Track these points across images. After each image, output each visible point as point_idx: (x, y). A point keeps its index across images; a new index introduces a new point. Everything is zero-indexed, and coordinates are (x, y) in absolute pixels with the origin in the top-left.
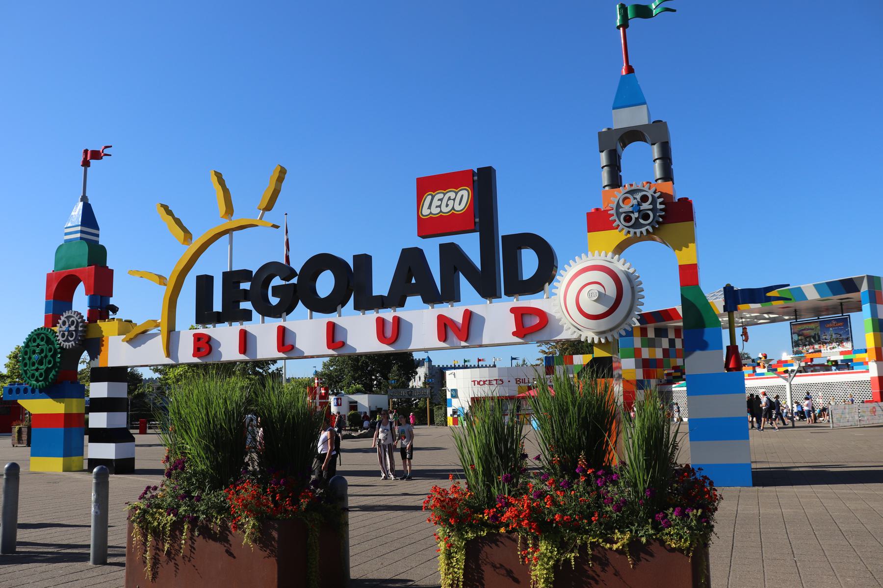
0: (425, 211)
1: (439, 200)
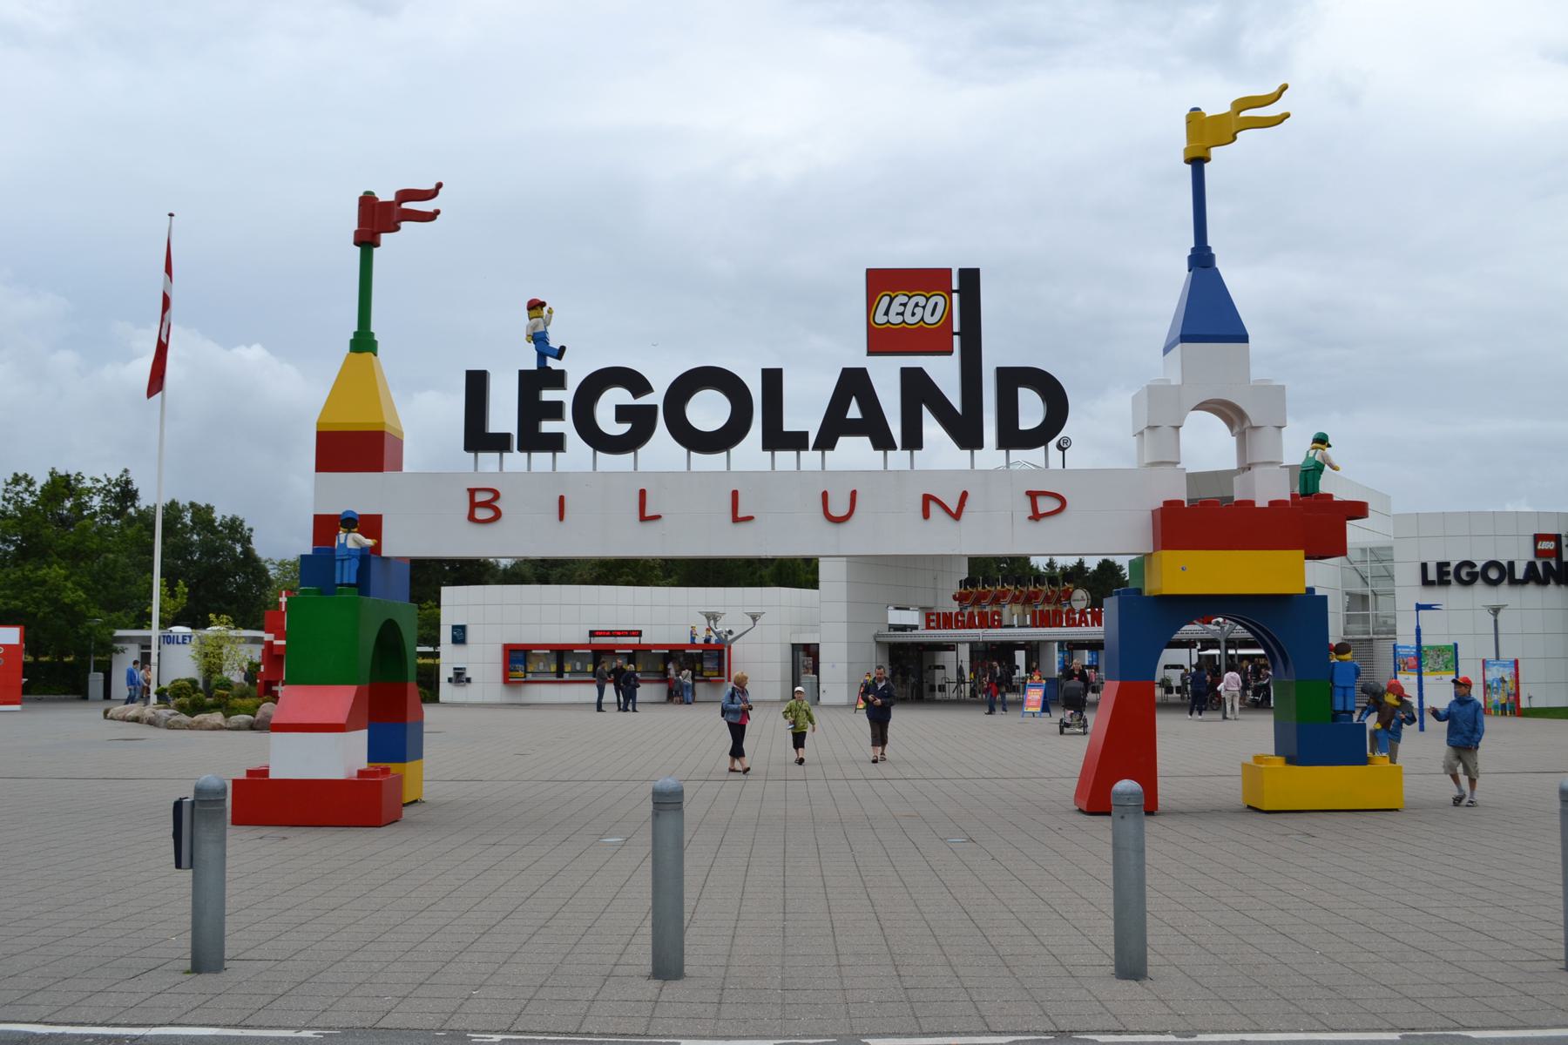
0: (880, 318)
1: (901, 304)
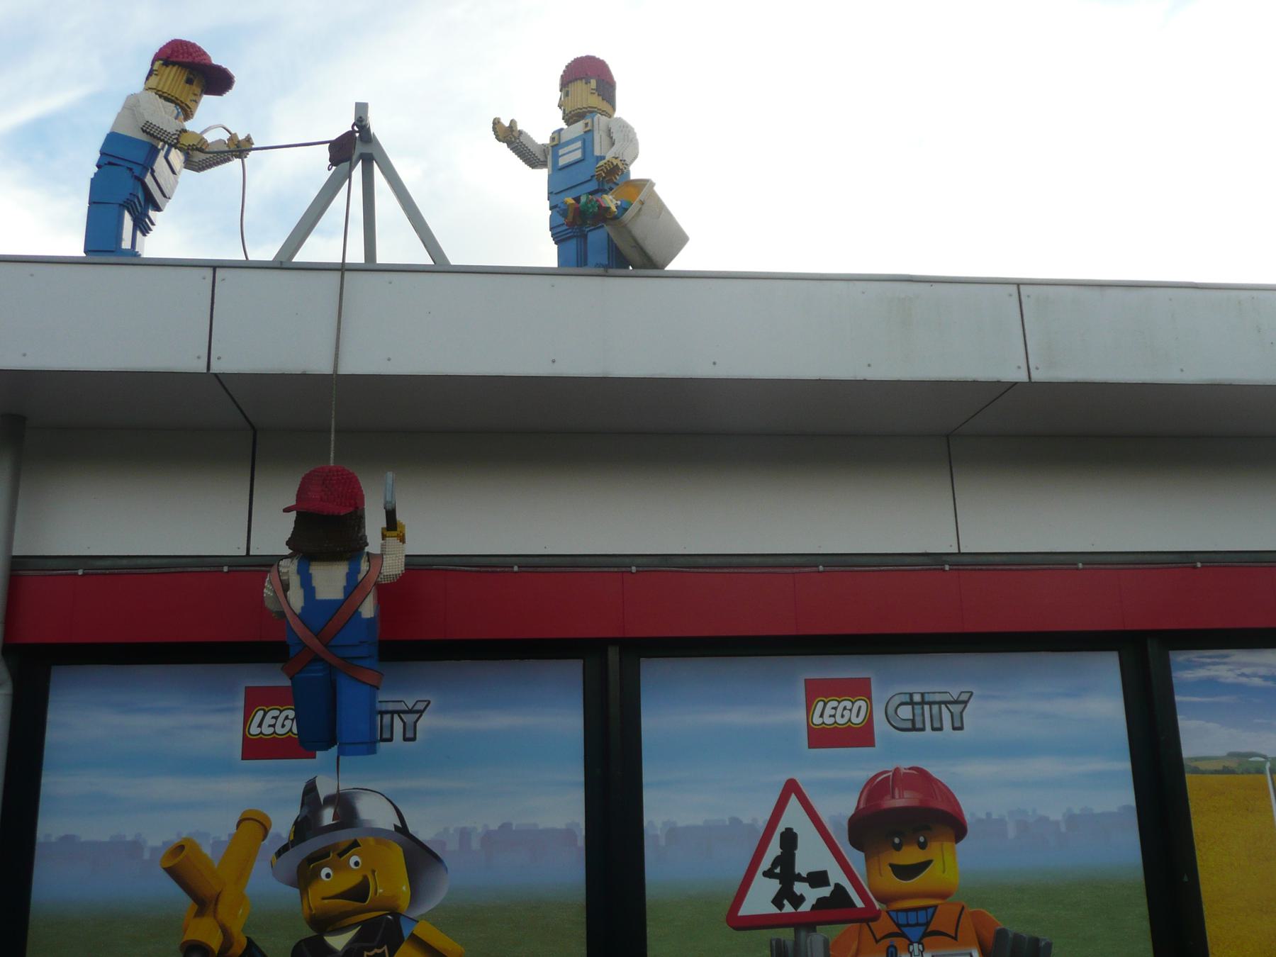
1: (833, 708)
